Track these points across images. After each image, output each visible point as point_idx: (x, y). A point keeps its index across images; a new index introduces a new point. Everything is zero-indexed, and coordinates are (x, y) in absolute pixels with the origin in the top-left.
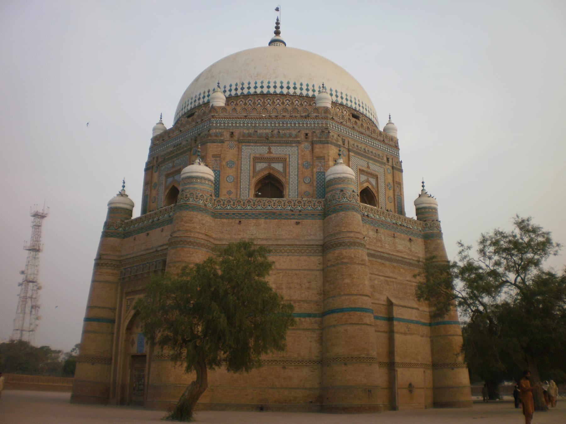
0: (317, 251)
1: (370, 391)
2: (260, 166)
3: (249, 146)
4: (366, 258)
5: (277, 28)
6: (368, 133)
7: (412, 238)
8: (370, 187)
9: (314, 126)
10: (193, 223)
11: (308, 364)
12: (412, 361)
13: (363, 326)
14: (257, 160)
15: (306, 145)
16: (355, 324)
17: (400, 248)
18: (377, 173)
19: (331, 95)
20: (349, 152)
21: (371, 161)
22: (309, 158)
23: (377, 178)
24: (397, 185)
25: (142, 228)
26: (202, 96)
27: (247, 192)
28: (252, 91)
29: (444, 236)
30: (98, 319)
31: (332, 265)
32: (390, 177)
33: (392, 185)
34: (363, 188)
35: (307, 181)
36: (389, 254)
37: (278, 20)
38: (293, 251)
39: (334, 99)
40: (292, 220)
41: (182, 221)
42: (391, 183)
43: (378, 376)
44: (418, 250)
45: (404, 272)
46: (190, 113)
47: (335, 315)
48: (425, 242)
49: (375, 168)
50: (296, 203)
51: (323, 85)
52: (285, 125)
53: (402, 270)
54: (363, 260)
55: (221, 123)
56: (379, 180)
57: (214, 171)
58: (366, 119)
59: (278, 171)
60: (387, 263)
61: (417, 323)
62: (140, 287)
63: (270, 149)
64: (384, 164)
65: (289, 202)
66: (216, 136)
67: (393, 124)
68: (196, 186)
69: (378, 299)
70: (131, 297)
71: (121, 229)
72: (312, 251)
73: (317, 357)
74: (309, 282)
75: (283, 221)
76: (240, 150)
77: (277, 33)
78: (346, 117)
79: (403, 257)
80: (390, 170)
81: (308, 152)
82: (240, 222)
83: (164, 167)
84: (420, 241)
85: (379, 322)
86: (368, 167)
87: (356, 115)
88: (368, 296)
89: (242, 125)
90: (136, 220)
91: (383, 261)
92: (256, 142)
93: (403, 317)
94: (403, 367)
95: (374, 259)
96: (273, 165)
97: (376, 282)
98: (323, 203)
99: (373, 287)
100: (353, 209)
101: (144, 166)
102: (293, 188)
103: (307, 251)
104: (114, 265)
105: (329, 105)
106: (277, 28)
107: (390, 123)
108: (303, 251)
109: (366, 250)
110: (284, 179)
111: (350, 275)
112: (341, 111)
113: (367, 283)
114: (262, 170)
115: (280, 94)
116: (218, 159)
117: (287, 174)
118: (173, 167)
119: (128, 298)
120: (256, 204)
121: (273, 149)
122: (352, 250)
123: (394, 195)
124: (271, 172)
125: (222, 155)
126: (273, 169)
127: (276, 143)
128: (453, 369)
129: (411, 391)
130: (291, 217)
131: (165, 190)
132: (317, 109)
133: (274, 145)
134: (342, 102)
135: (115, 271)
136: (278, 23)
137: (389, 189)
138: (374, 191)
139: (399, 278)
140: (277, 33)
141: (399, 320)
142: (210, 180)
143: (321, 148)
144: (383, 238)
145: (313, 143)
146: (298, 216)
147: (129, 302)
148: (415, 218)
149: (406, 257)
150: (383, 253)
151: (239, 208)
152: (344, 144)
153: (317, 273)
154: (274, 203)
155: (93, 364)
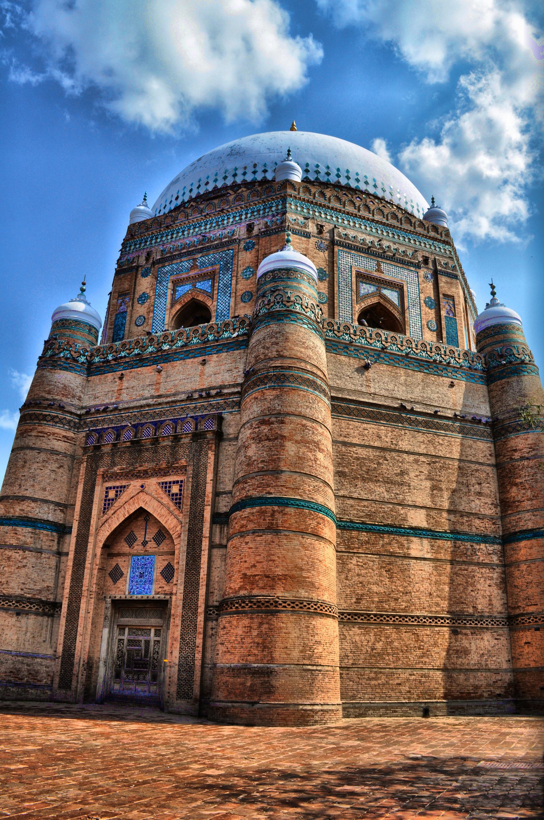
10: (306, 348)
14: (362, 277)
31: (522, 458)
41: (287, 339)
63: (379, 265)
73: (501, 613)
74: (480, 484)
83: (167, 268)
98: (483, 359)
114: (368, 296)
124: (382, 301)
131: (173, 305)
135: (71, 434)
153: (489, 469)
155: (18, 614)
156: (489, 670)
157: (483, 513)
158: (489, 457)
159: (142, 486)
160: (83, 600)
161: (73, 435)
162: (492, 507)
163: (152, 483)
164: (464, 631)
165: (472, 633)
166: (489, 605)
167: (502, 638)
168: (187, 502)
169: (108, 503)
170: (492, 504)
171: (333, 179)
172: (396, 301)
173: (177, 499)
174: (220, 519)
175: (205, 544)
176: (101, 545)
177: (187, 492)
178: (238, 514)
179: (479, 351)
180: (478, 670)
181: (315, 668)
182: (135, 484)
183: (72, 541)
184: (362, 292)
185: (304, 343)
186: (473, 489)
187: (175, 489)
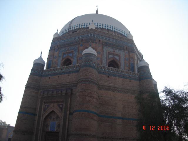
10: (93, 73)
14: (109, 53)
15: (126, 52)
25: (54, 74)
35: (127, 65)
37: (97, 9)
59: (117, 60)
62: (55, 100)
68: (92, 58)
71: (40, 73)
90: (45, 70)
119: (45, 104)
121: (115, 50)
124: (114, 59)
126: (115, 58)
131: (63, 59)
147: (46, 107)
159: (53, 105)
160: (40, 132)
163: (56, 104)
168: (63, 109)
169: (45, 109)
171: (104, 27)
173: (61, 109)
174: (71, 114)
175: (67, 120)
177: (64, 107)
178: (74, 113)
179: (138, 72)
182: (52, 105)
183: (37, 118)
187: (61, 106)
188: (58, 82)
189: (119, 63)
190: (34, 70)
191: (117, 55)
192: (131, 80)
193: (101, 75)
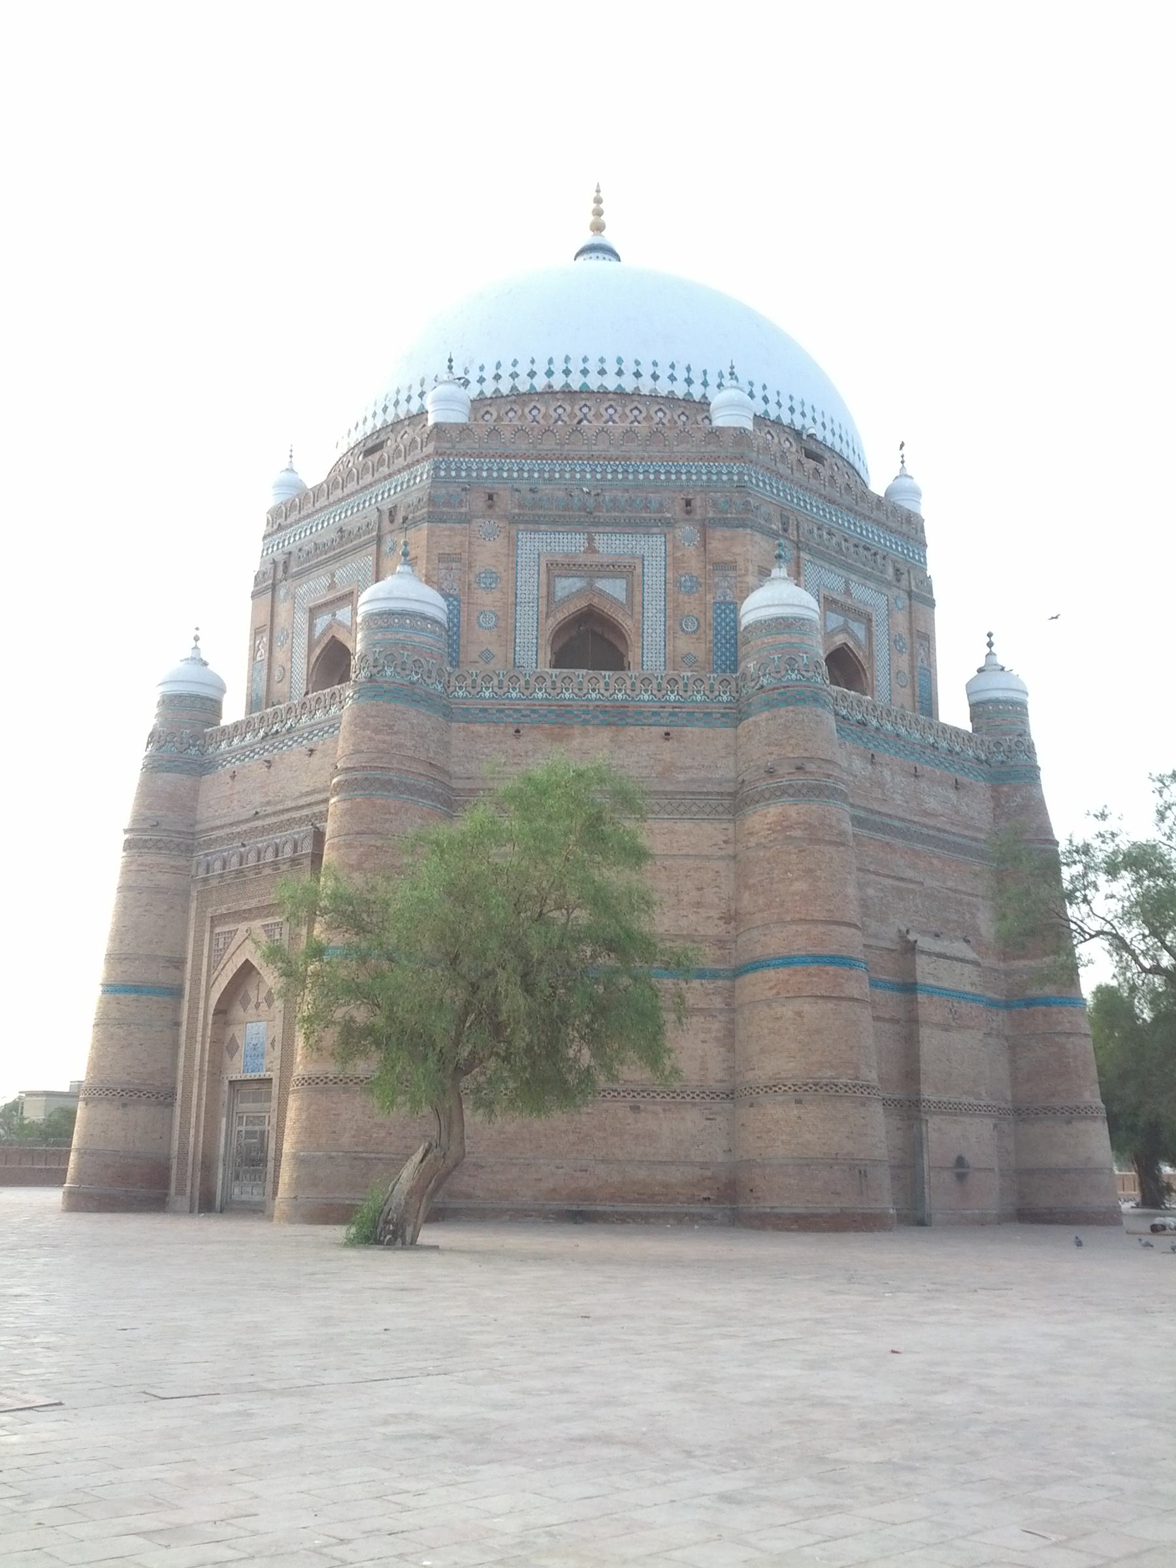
0: (720, 809)
1: (863, 1174)
2: (566, 586)
3: (536, 531)
4: (848, 826)
5: (598, 213)
6: (847, 499)
7: (965, 780)
8: (851, 644)
9: (709, 479)
11: (698, 1100)
12: (965, 1099)
13: (844, 1003)
14: (556, 569)
15: (687, 531)
16: (822, 997)
17: (931, 804)
18: (869, 610)
19: (751, 395)
20: (798, 549)
21: (853, 577)
22: (694, 565)
23: (870, 620)
24: (920, 640)
26: (403, 397)
27: (532, 654)
28: (540, 383)
29: (1043, 775)
30: (136, 989)
32: (901, 618)
33: (907, 640)
34: (832, 648)
36: (903, 820)
38: (657, 808)
39: (759, 407)
40: (653, 729)
42: (906, 636)
43: (877, 1132)
44: (976, 807)
45: (940, 866)
46: (370, 444)
47: (771, 974)
48: (995, 789)
49: (864, 594)
50: (664, 685)
51: (732, 367)
52: (631, 477)
53: (935, 861)
54: (842, 833)
55: (458, 469)
56: (874, 629)
57: (446, 596)
58: (840, 463)
59: (614, 601)
60: (899, 842)
61: (975, 998)
62: (253, 903)
63: (591, 540)
64: (889, 584)
65: (646, 680)
66: (447, 504)
67: (911, 477)
69: (875, 936)
70: (226, 928)
71: (193, 751)
72: (708, 810)
73: (721, 1081)
74: (700, 889)
75: (631, 731)
76: (513, 543)
77: (598, 228)
78: (792, 458)
79: (939, 830)
80: (903, 601)
81: (690, 550)
82: (518, 731)
84: (982, 787)
85: (880, 995)
86: (848, 592)
87: (814, 452)
88: (856, 926)
89: (515, 475)
91: (888, 838)
92: (554, 522)
93: (940, 984)
94: (942, 1113)
95: (865, 832)
96: (601, 584)
97: (871, 892)
98: (733, 684)
99: (864, 904)
100: (816, 700)
101: (250, 587)
102: (651, 644)
103: (694, 809)
104: (178, 845)
105: (749, 425)
106: (598, 213)
107: (903, 475)
108: (682, 809)
109: (848, 808)
110: (629, 622)
111: (811, 871)
112: (776, 440)
113: (851, 891)
114: (569, 598)
115: (615, 393)
116: (454, 565)
117: (638, 609)
118: (332, 586)
119: (218, 930)
120: (558, 685)
121: (601, 542)
122: (814, 808)
123: (912, 667)
124: (596, 600)
125: (465, 556)
126: (601, 593)
127: (605, 524)
128: (1069, 1122)
129: (961, 1177)
130: (651, 721)
132: (716, 434)
133: (601, 529)
134: (778, 417)
136: (598, 201)
137: (901, 651)
138: (860, 655)
139: (928, 882)
140: (598, 228)
141: (932, 991)
142: (435, 621)
143: (725, 539)
144: (889, 779)
145: (704, 527)
146: (672, 721)
148: (966, 725)
149: (948, 827)
150: (889, 816)
151: (514, 695)
152: (785, 530)
154: (607, 684)
156: (692, 1163)
157: (702, 933)
158: (724, 846)
161: (185, 863)
162: (721, 923)
163: (257, 924)
164: (651, 1108)
165: (664, 1110)
166: (702, 1069)
167: (719, 1118)
170: (721, 918)
172: (621, 596)
176: (211, 1011)
180: (673, 1163)
181: (373, 1155)
182: (243, 927)
184: (560, 594)
185: (391, 727)
186: (686, 898)
188: (266, 795)
189: (627, 624)
190: (156, 738)
191: (614, 569)
192: (674, 731)
193: (473, 728)
